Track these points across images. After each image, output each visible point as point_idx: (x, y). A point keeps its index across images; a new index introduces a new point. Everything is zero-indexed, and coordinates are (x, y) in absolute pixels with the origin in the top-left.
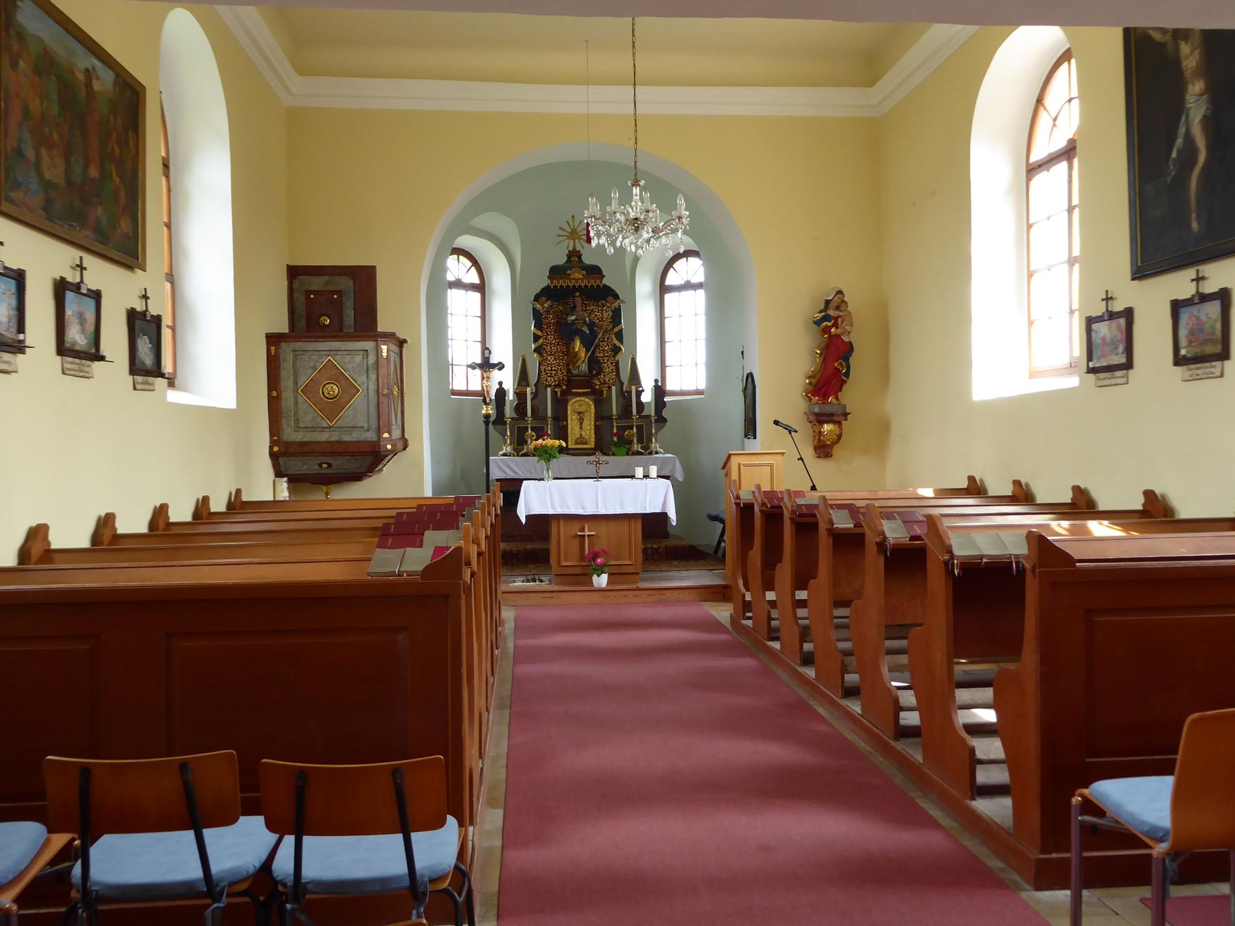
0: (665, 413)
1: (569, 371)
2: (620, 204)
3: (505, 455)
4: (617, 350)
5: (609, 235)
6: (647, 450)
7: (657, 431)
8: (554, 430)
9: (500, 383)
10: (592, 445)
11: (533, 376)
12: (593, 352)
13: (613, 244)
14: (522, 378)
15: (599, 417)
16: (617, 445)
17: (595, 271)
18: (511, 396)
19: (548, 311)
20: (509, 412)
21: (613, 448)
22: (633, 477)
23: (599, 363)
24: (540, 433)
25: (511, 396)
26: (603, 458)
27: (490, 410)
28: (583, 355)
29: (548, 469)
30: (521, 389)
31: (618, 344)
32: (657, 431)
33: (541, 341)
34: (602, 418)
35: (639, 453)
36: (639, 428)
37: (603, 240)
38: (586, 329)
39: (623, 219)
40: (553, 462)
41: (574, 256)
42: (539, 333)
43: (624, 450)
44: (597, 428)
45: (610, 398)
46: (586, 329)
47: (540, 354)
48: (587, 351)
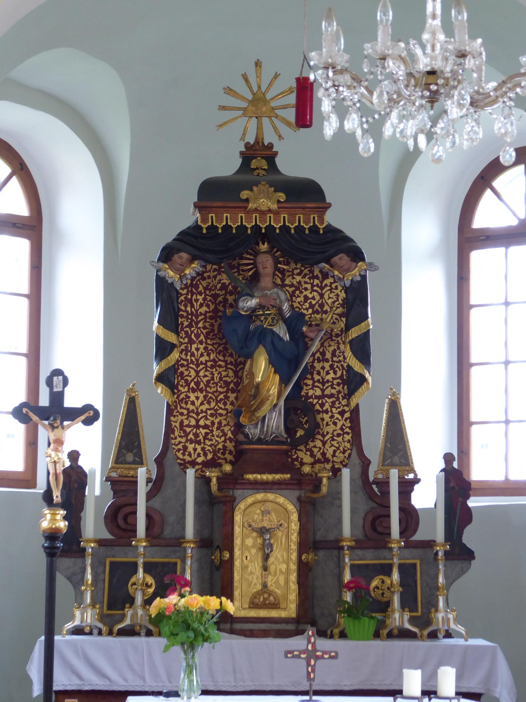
0: (470, 537)
1: (239, 428)
2: (396, 39)
3: (78, 631)
4: (354, 382)
5: (365, 111)
6: (424, 627)
7: (450, 581)
8: (199, 571)
9: (74, 456)
10: (290, 609)
11: (152, 441)
12: (298, 387)
13: (374, 130)
14: (128, 444)
15: (308, 543)
16: (352, 612)
17: (307, 193)
18: (96, 488)
19: (192, 286)
20: (92, 526)
21: (343, 621)
22: (396, 693)
23: (309, 410)
24: (166, 580)
25: (96, 488)
26: (323, 644)
27: (56, 520)
28: (274, 391)
29: (190, 669)
30: (123, 470)
31: (357, 366)
32: (450, 581)
33: (175, 355)
34: (315, 543)
35: (404, 634)
36: (407, 571)
37: (353, 123)
38: (281, 331)
39: (401, 72)
40: (203, 651)
41: (258, 156)
42: (171, 338)
43: (368, 624)
44: (304, 570)
45: (337, 495)
46: (281, 331)
47: (172, 387)
48: (284, 381)
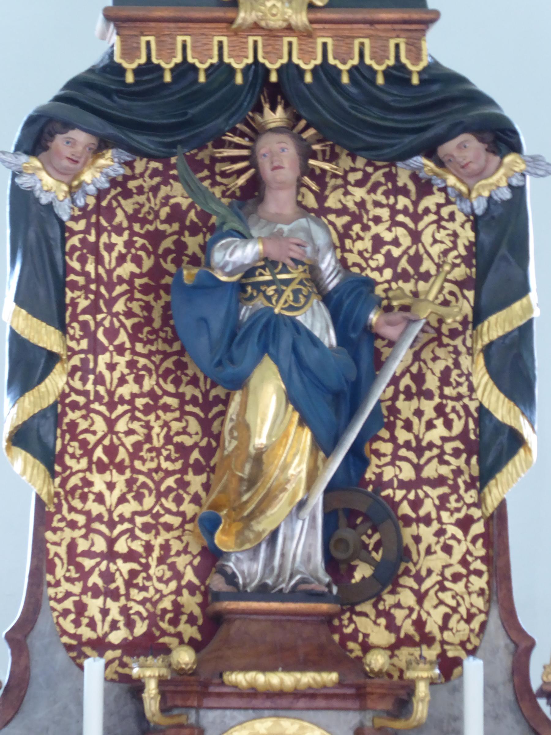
1: (212, 558)
12: (358, 458)
19: (99, 212)
23: (382, 515)
28: (299, 468)
31: (503, 409)
33: (56, 381)
38: (317, 321)
42: (47, 337)
47: (50, 459)
48: (325, 445)
